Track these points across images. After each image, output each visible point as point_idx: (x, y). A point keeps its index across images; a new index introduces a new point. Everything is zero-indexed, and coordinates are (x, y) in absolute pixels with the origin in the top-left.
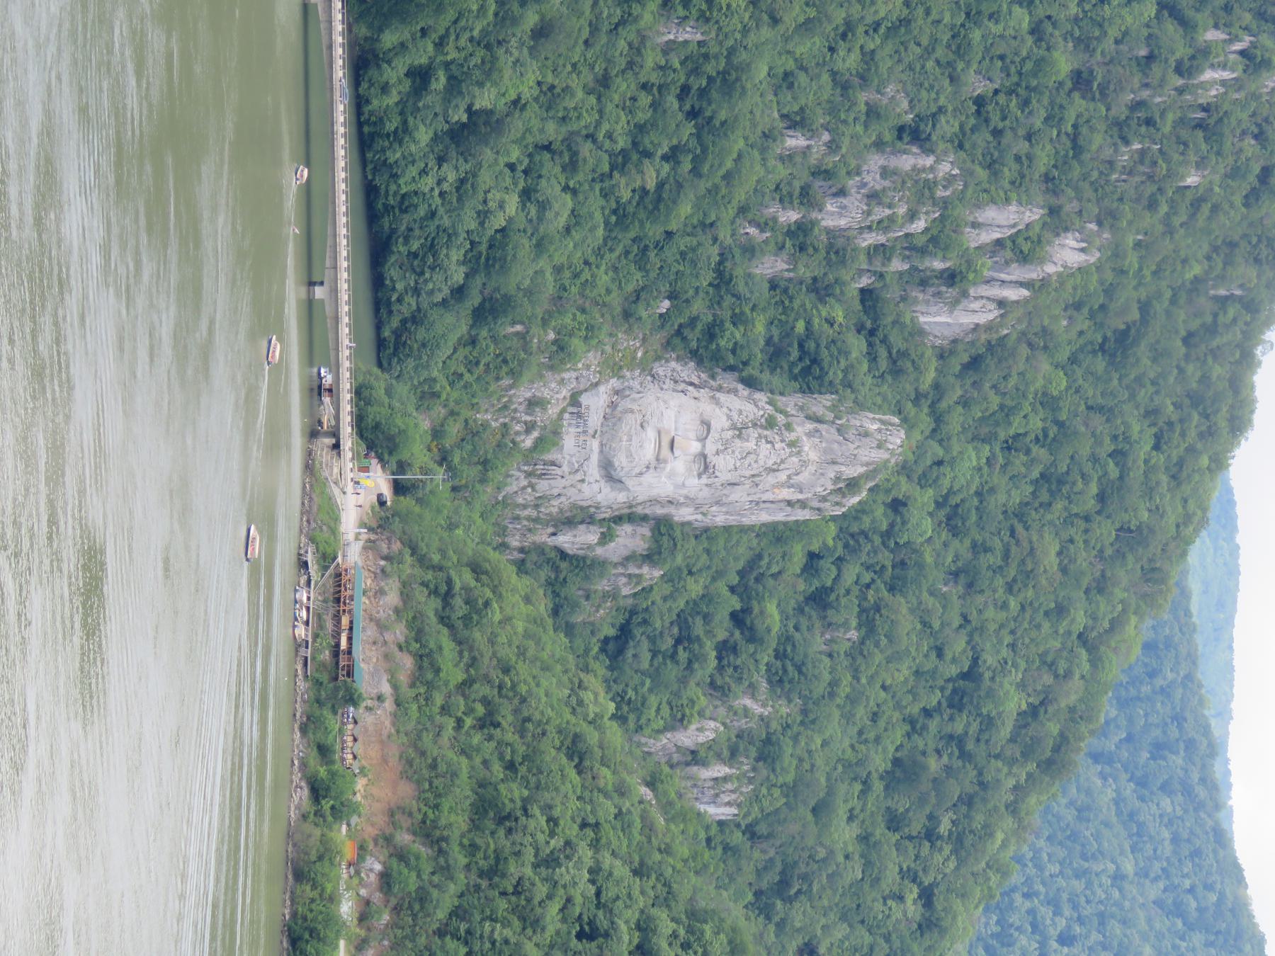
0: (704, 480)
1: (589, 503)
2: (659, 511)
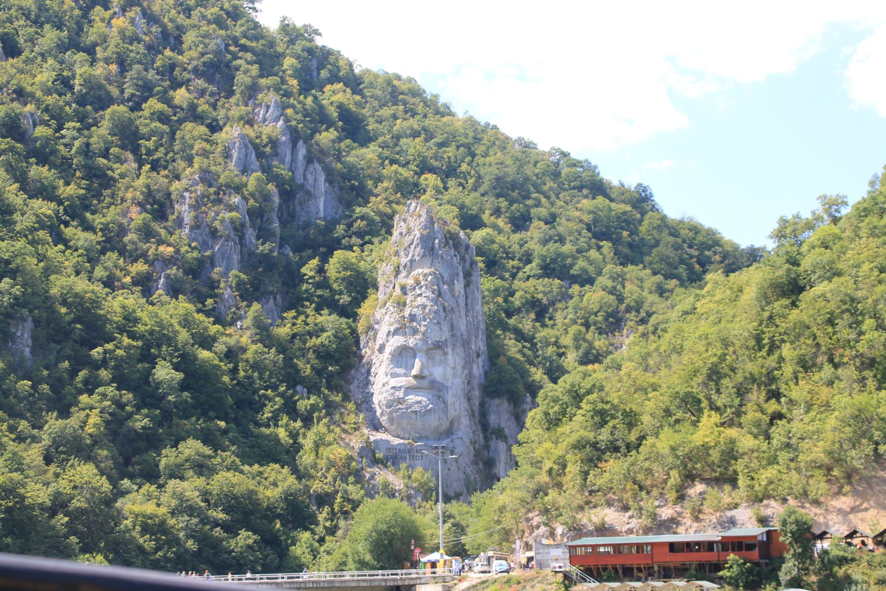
0: (450, 350)
1: (471, 448)
2: (477, 393)
